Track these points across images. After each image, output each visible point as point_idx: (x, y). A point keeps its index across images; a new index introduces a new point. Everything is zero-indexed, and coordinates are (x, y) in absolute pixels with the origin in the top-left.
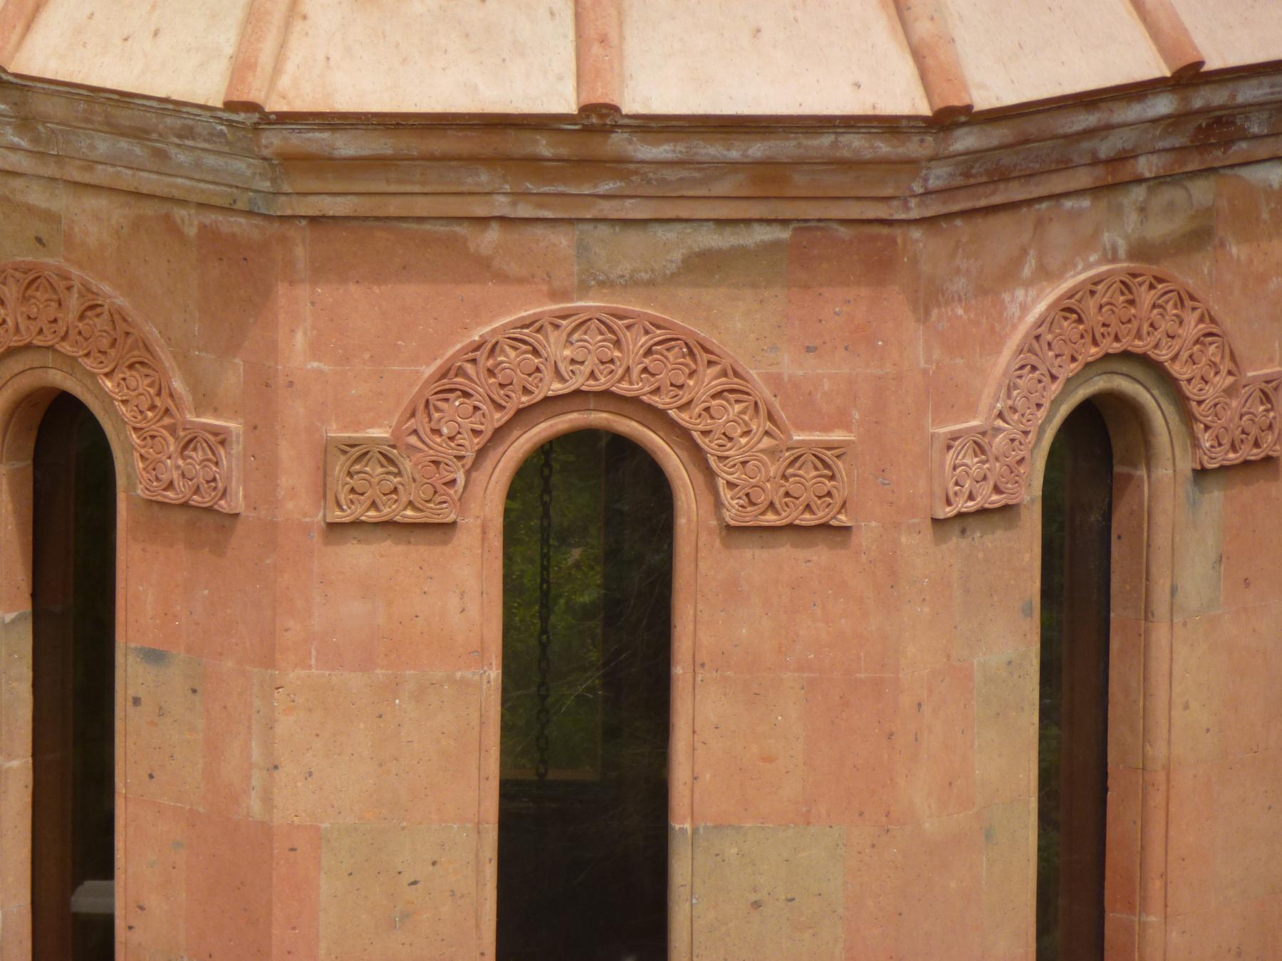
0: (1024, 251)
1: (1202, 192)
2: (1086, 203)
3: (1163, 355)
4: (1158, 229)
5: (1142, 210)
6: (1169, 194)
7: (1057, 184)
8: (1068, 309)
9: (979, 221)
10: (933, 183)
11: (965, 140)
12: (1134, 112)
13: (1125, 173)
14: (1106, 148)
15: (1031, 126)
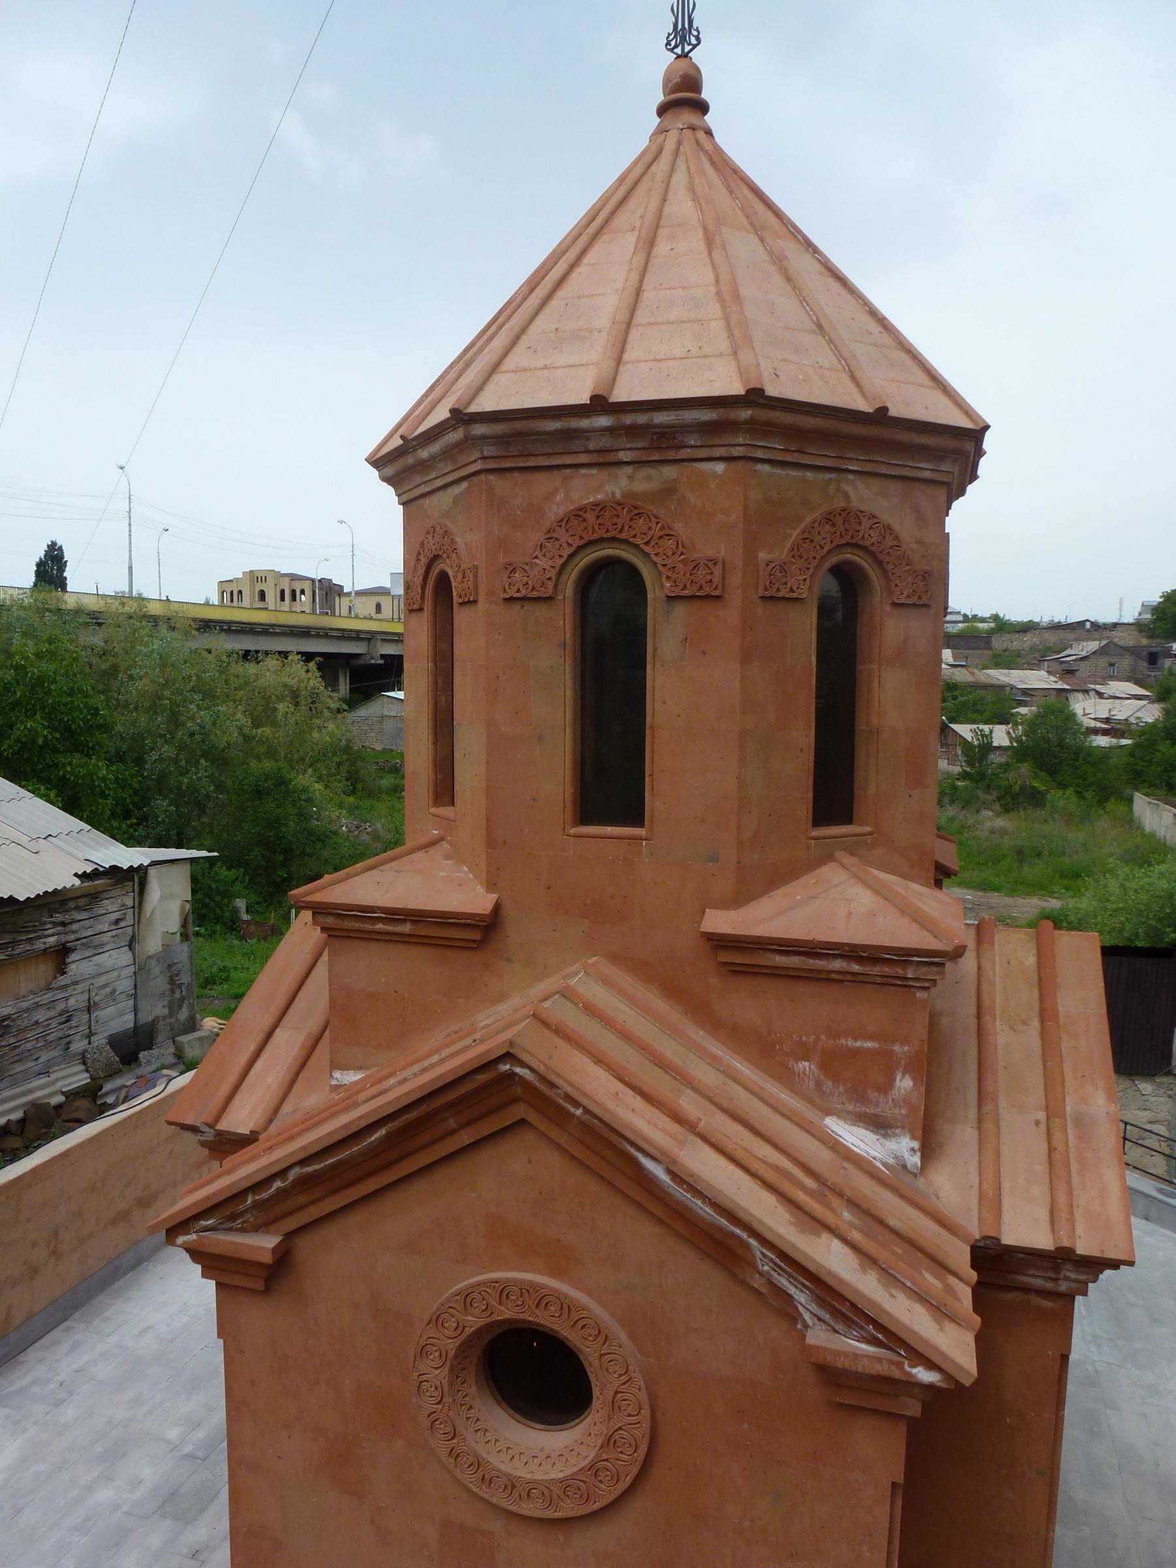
0: (556, 491)
1: (669, 472)
2: (594, 471)
3: (638, 541)
4: (641, 486)
5: (631, 477)
6: (646, 471)
7: (568, 460)
8: (579, 513)
9: (530, 476)
10: (486, 453)
11: (479, 430)
12: (584, 423)
13: (612, 457)
14: (592, 446)
15: (520, 425)
